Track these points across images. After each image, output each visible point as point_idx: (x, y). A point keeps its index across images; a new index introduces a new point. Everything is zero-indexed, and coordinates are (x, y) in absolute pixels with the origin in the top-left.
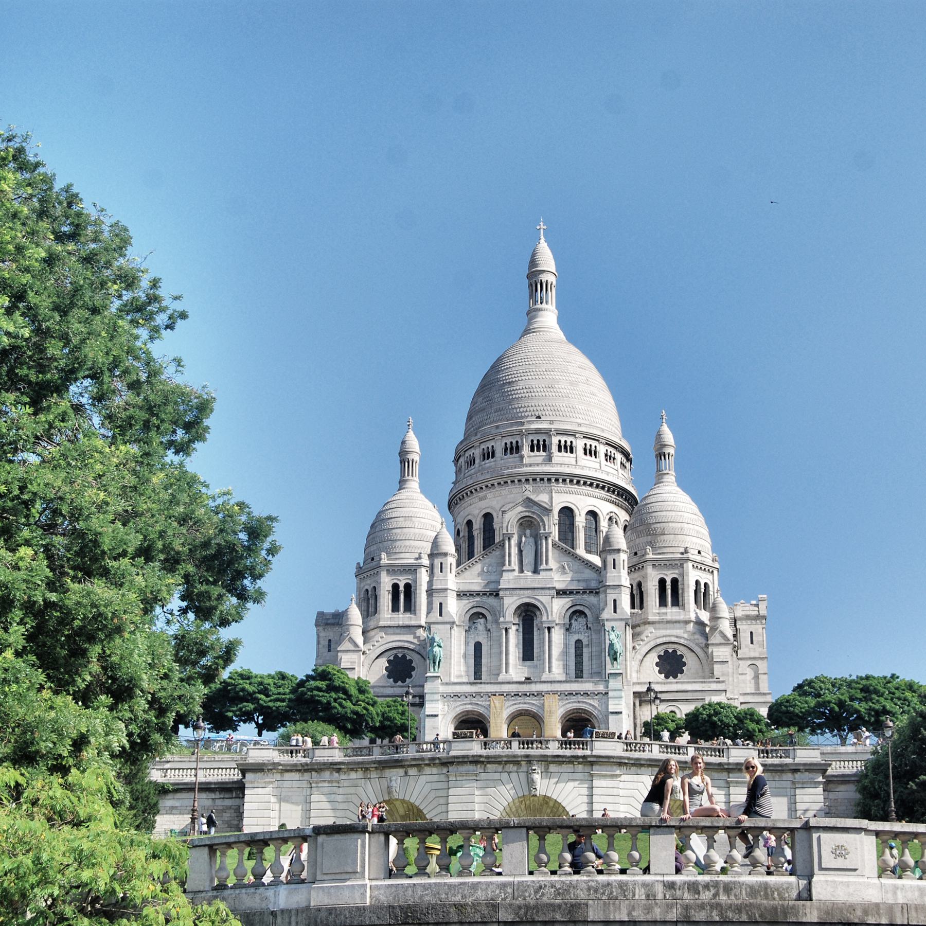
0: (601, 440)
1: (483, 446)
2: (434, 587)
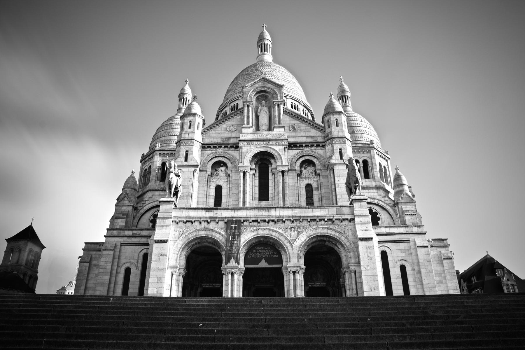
0: (301, 103)
1: (232, 105)
2: (182, 138)
